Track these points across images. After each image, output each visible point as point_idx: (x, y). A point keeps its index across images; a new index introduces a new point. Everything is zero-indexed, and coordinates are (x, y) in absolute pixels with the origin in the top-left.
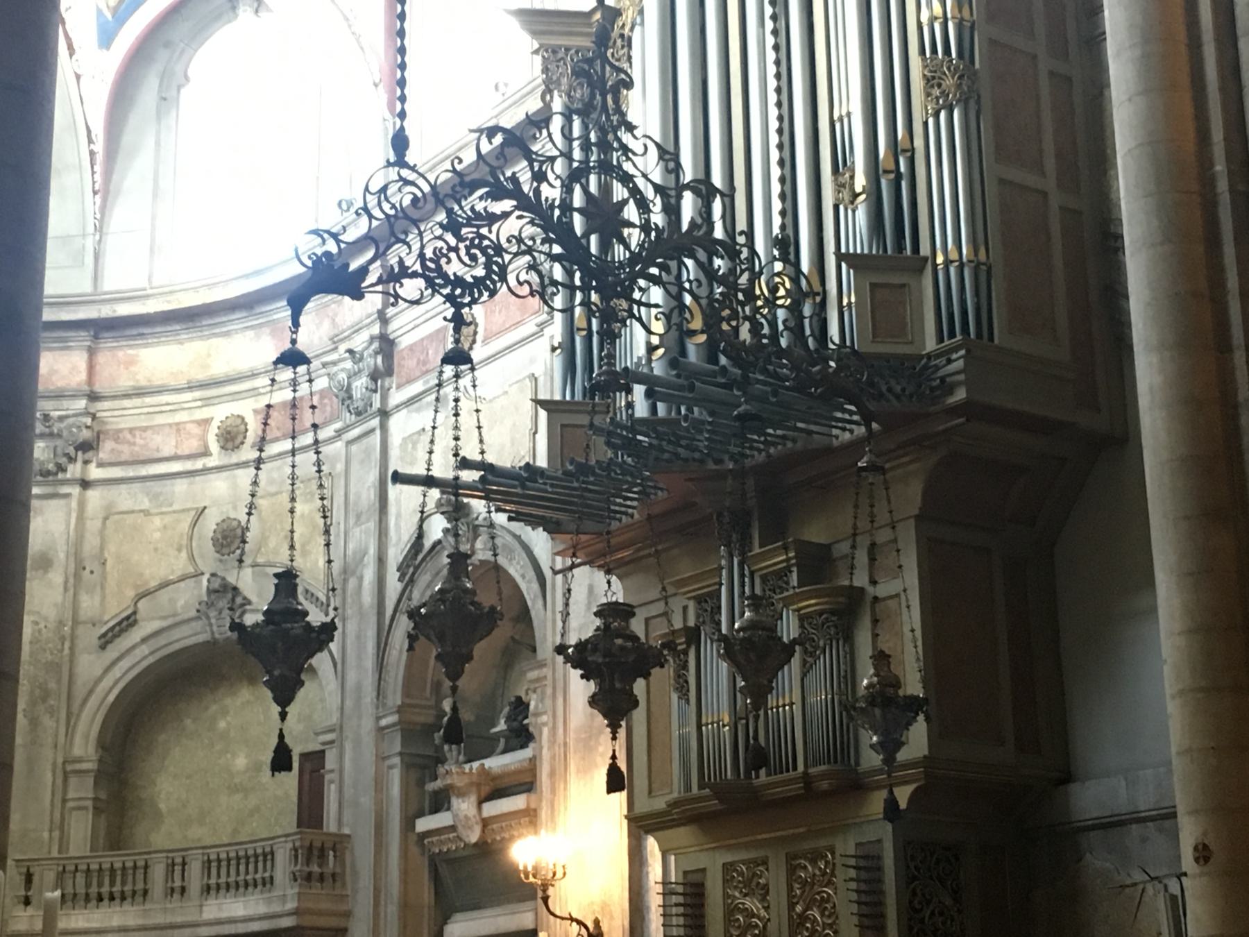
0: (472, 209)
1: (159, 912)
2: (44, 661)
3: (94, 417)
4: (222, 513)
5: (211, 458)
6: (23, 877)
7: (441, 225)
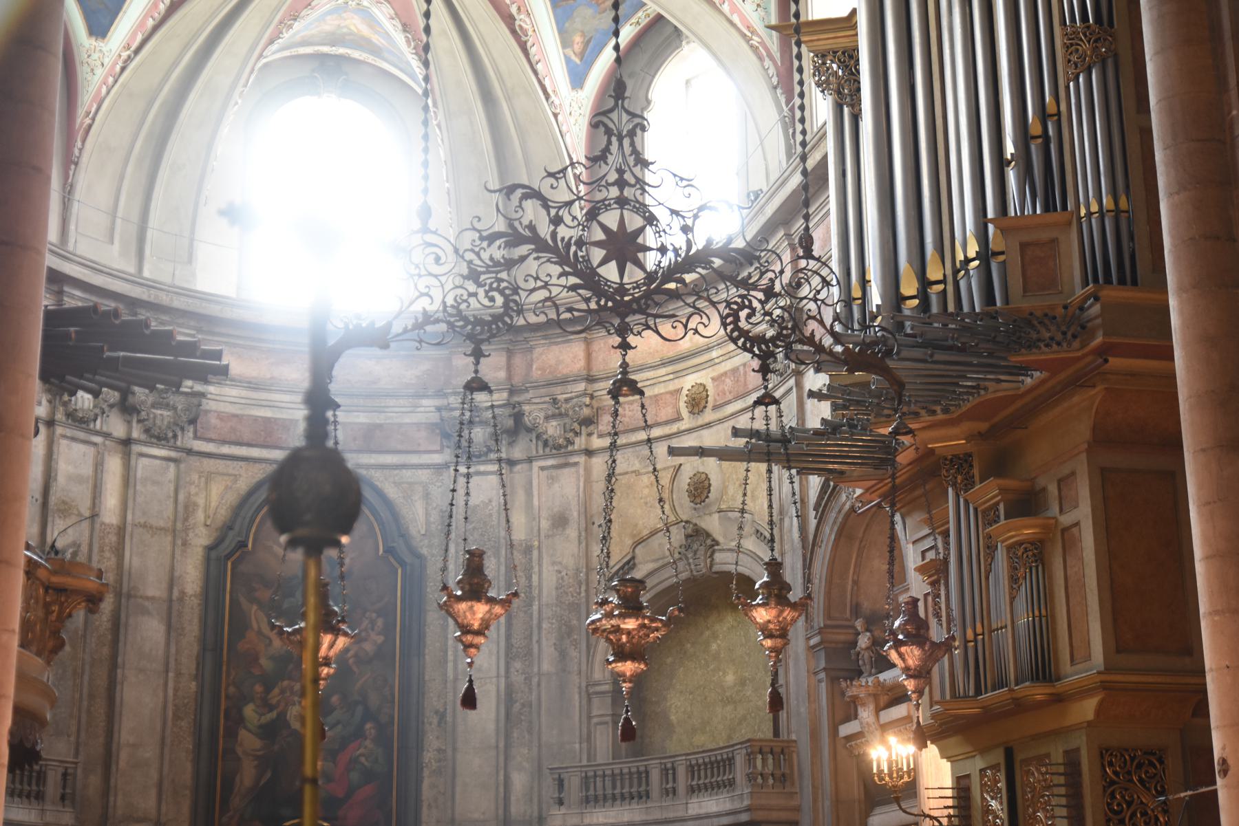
0: (491, 259)
1: (656, 810)
2: (567, 602)
3: (592, 397)
4: (694, 467)
5: (684, 422)
6: (556, 782)
7: (464, 278)
